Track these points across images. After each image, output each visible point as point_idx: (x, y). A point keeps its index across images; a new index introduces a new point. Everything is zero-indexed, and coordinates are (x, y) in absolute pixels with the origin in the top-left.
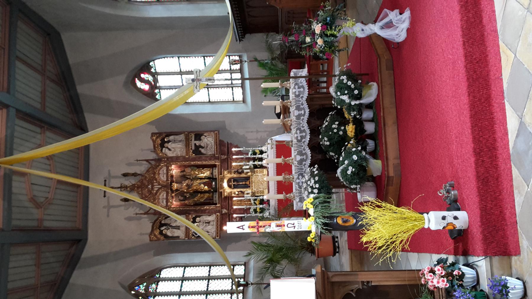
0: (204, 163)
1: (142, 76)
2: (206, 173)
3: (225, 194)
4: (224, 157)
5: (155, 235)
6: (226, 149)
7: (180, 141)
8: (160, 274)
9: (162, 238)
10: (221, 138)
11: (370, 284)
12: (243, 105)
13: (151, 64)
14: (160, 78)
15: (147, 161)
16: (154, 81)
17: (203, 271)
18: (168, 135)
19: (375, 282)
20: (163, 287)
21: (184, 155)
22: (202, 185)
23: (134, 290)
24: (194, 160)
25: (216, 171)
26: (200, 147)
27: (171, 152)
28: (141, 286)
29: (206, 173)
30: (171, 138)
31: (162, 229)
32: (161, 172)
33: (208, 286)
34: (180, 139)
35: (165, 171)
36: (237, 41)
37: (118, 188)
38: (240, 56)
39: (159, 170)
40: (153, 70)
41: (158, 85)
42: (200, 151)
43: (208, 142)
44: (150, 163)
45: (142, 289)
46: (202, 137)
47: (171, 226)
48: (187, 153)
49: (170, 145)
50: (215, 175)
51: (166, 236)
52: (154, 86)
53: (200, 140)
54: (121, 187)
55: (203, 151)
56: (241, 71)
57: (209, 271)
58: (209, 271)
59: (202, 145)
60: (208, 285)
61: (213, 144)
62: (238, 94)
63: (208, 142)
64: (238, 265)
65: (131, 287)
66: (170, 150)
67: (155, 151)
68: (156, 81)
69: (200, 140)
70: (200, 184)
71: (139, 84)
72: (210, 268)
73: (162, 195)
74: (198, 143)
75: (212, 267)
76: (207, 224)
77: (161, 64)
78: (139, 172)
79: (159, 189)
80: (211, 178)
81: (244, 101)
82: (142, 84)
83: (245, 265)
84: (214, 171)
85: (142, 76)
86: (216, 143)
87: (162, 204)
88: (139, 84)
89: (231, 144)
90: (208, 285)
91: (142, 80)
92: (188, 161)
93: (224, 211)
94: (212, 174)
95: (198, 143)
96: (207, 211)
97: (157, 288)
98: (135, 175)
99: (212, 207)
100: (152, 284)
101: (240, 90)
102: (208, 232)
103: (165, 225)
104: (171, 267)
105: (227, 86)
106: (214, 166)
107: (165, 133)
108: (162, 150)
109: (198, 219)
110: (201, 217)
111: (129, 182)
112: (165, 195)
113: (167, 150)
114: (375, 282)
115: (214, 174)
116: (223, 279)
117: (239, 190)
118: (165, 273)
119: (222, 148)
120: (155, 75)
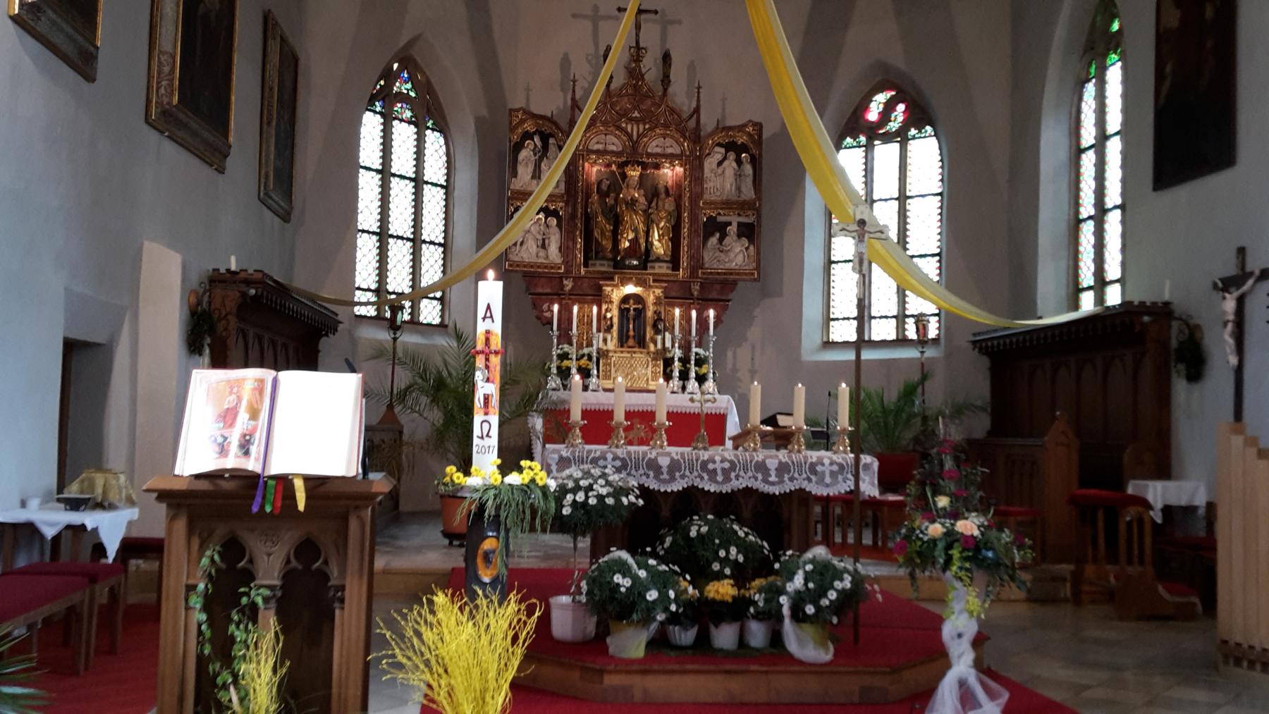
0: (685, 243)
1: (901, 107)
2: (659, 246)
3: (609, 289)
4: (696, 289)
5: (522, 122)
6: (714, 295)
7: (739, 189)
8: (433, 130)
9: (515, 138)
10: (740, 284)
11: (337, 605)
12: (819, 342)
13: (928, 128)
14: (894, 148)
15: (697, 110)
16: (887, 133)
17: (433, 228)
18: (755, 161)
19: (342, 616)
20: (404, 134)
21: (706, 197)
22: (631, 236)
23: (400, 70)
24: (694, 218)
25: (662, 269)
27: (714, 166)
28: (409, 86)
29: (659, 246)
30: (748, 169)
31: (536, 139)
32: (669, 141)
33: (398, 237)
34: (743, 189)
35: (670, 151)
36: (974, 335)
37: (637, 42)
38: (936, 341)
39: (672, 137)
40: (913, 132)
41: (876, 142)
42: (712, 234)
43: (732, 255)
44: (691, 116)
45: (404, 87)
46: (745, 241)
47: (540, 160)
48: (710, 204)
49: (730, 164)
50: (653, 268)
51: (518, 147)
52: (874, 133)
53: (739, 236)
54: (638, 47)
55: (714, 240)
56: (902, 341)
57: (432, 243)
58: (432, 243)
59: (727, 241)
60: (402, 238)
61: (727, 266)
63: (736, 255)
64: (442, 310)
65: (408, 62)
66: (720, 163)
67: (721, 128)
68: (888, 138)
69: (739, 236)
70: (636, 230)
71: (881, 98)
72: (440, 245)
73: (615, 140)
74: (733, 229)
75: (441, 249)
76: (540, 243)
77: (926, 152)
78: (670, 90)
79: (630, 136)
80: (646, 257)
81: (828, 344)
82: (881, 106)
83: (442, 325)
84: (664, 265)
85: (901, 107)
86: (730, 272)
87: (595, 140)
88: (881, 98)
89: (726, 308)
90: (402, 238)
91: (889, 107)
92: (691, 204)
93: (568, 284)
94: (658, 260)
95: (733, 229)
96: (571, 244)
97: (402, 120)
98: (666, 80)
99: (580, 257)
100: (412, 110)
102: (522, 243)
103: (545, 147)
104: (448, 154)
106: (676, 267)
107: (760, 155)
108: (719, 145)
109: (553, 221)
110: (557, 230)
111: (651, 67)
112: (614, 148)
113: (719, 157)
114: (342, 616)
115: (657, 265)
116: (413, 273)
117: (615, 320)
118: (434, 141)
119: (718, 287)
120: (902, 137)
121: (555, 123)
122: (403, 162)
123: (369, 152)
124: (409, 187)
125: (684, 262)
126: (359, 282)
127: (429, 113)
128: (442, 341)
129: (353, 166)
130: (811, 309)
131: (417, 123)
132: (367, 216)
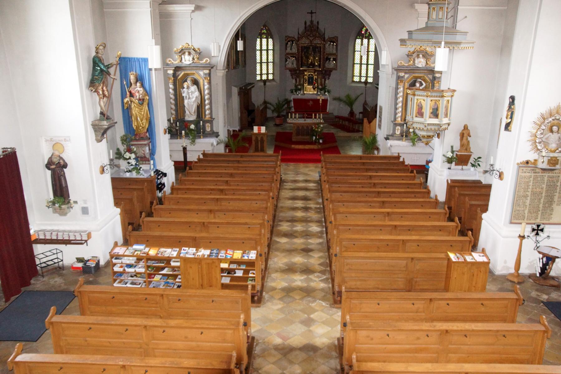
4: (324, 72)
17: (271, 59)
20: (264, 41)
45: (265, 31)
51: (287, 44)
55: (328, 62)
62: (356, 79)
65: (265, 26)
67: (329, 38)
81: (353, 81)
83: (273, 79)
93: (298, 72)
98: (318, 28)
101: (358, 80)
103: (293, 43)
105: (360, 74)
111: (315, 23)
118: (270, 41)
121: (294, 38)
122: (264, 47)
123: (258, 47)
124: (266, 52)
125: (321, 67)
126: (257, 73)
127: (269, 35)
129: (255, 50)
130: (349, 74)
131: (267, 38)
132: (258, 60)
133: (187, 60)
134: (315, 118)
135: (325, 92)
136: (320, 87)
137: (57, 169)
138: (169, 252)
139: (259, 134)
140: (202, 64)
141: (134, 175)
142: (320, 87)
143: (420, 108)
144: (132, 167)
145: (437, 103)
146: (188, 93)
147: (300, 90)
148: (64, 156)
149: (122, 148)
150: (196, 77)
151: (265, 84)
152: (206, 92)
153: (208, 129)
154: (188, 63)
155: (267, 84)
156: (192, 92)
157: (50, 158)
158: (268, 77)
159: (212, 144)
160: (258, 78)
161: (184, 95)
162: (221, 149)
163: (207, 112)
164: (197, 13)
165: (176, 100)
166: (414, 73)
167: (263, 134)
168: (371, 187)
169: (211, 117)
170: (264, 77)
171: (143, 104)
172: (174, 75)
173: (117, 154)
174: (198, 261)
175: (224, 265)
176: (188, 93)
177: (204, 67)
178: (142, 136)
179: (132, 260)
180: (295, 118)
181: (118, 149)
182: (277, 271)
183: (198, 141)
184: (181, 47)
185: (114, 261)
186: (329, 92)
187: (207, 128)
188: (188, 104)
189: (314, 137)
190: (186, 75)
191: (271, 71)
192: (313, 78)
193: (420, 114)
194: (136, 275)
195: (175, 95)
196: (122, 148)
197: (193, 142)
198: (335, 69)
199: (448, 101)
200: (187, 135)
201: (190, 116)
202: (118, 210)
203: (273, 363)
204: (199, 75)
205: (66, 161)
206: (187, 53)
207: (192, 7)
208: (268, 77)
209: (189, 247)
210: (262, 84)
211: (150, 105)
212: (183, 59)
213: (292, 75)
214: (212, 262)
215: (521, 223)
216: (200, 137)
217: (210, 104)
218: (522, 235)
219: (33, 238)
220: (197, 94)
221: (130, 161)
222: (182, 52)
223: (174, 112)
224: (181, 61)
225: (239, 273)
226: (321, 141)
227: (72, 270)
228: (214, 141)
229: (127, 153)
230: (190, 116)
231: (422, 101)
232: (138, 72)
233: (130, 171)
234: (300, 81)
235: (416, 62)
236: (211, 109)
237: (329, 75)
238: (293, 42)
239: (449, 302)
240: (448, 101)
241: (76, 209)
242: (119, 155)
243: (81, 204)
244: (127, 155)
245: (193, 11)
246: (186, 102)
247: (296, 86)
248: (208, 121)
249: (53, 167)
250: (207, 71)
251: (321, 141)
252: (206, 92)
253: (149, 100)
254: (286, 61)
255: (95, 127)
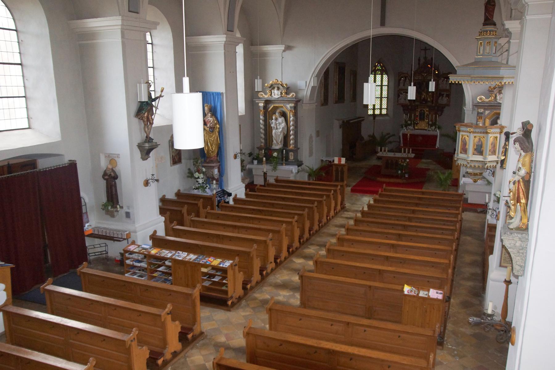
2: (429, 100)
4: (436, 108)
20: (378, 77)
26: (443, 97)
45: (379, 68)
51: (400, 80)
53: (446, 97)
55: (440, 98)
74: (445, 95)
80: (426, 101)
93: (410, 107)
95: (445, 95)
118: (385, 77)
128: (387, 118)
131: (382, 74)
133: (276, 94)
134: (405, 152)
135: (436, 128)
136: (430, 123)
137: (111, 179)
138: (204, 260)
139: (339, 165)
140: (289, 98)
141: (199, 192)
142: (430, 123)
143: (464, 144)
144: (199, 185)
145: (481, 139)
146: (276, 124)
147: (410, 125)
148: (116, 169)
149: (193, 169)
150: (284, 109)
151: (374, 119)
152: (292, 123)
153: (291, 157)
154: (276, 97)
155: (377, 118)
156: (280, 124)
157: (105, 171)
158: (381, 112)
159: (292, 172)
160: (370, 112)
161: (272, 125)
162: (305, 177)
163: (292, 142)
164: (287, 52)
165: (265, 130)
166: (495, 109)
167: (343, 165)
168: (406, 221)
169: (295, 147)
170: (377, 112)
171: (212, 132)
172: (265, 108)
173: (189, 173)
174: (183, 263)
175: (204, 270)
176: (276, 124)
177: (289, 102)
178: (212, 159)
179: (140, 257)
180: (385, 151)
181: (189, 169)
182: (271, 285)
183: (280, 167)
184: (271, 82)
185: (127, 255)
186: (439, 128)
187: (290, 156)
188: (275, 134)
189: (400, 172)
190: (275, 108)
191: (384, 106)
192: (424, 113)
193: (465, 151)
194: (140, 269)
195: (265, 125)
196: (193, 169)
197: (275, 169)
198: (448, 105)
199: (496, 137)
200: (268, 161)
201: (277, 145)
202: (163, 219)
203: (203, 356)
204: (287, 108)
205: (117, 174)
206: (276, 88)
207: (282, 47)
208: (381, 112)
209: (183, 251)
210: (372, 118)
211: (221, 133)
212: (273, 94)
213: (404, 110)
214: (195, 266)
215: (506, 267)
216: (282, 164)
217: (296, 134)
218: (507, 280)
219: (86, 234)
220: (283, 124)
221: (198, 180)
222: (272, 87)
223: (263, 141)
224: (271, 95)
225: (216, 279)
226: (407, 176)
227: (114, 262)
228: (294, 169)
229: (197, 173)
230: (277, 145)
231: (466, 137)
232: (213, 105)
233: (197, 189)
234: (411, 117)
235: (498, 97)
236: (296, 139)
237: (442, 111)
238: (406, 78)
239: (366, 329)
240: (496, 137)
241: (122, 212)
242: (190, 175)
243: (125, 209)
244: (197, 175)
245: (284, 51)
246: (274, 131)
247: (406, 122)
248: (291, 151)
249: (106, 177)
250: (293, 105)
251: (407, 176)
252: (292, 123)
253: (219, 128)
254: (399, 96)
255: (140, 146)
